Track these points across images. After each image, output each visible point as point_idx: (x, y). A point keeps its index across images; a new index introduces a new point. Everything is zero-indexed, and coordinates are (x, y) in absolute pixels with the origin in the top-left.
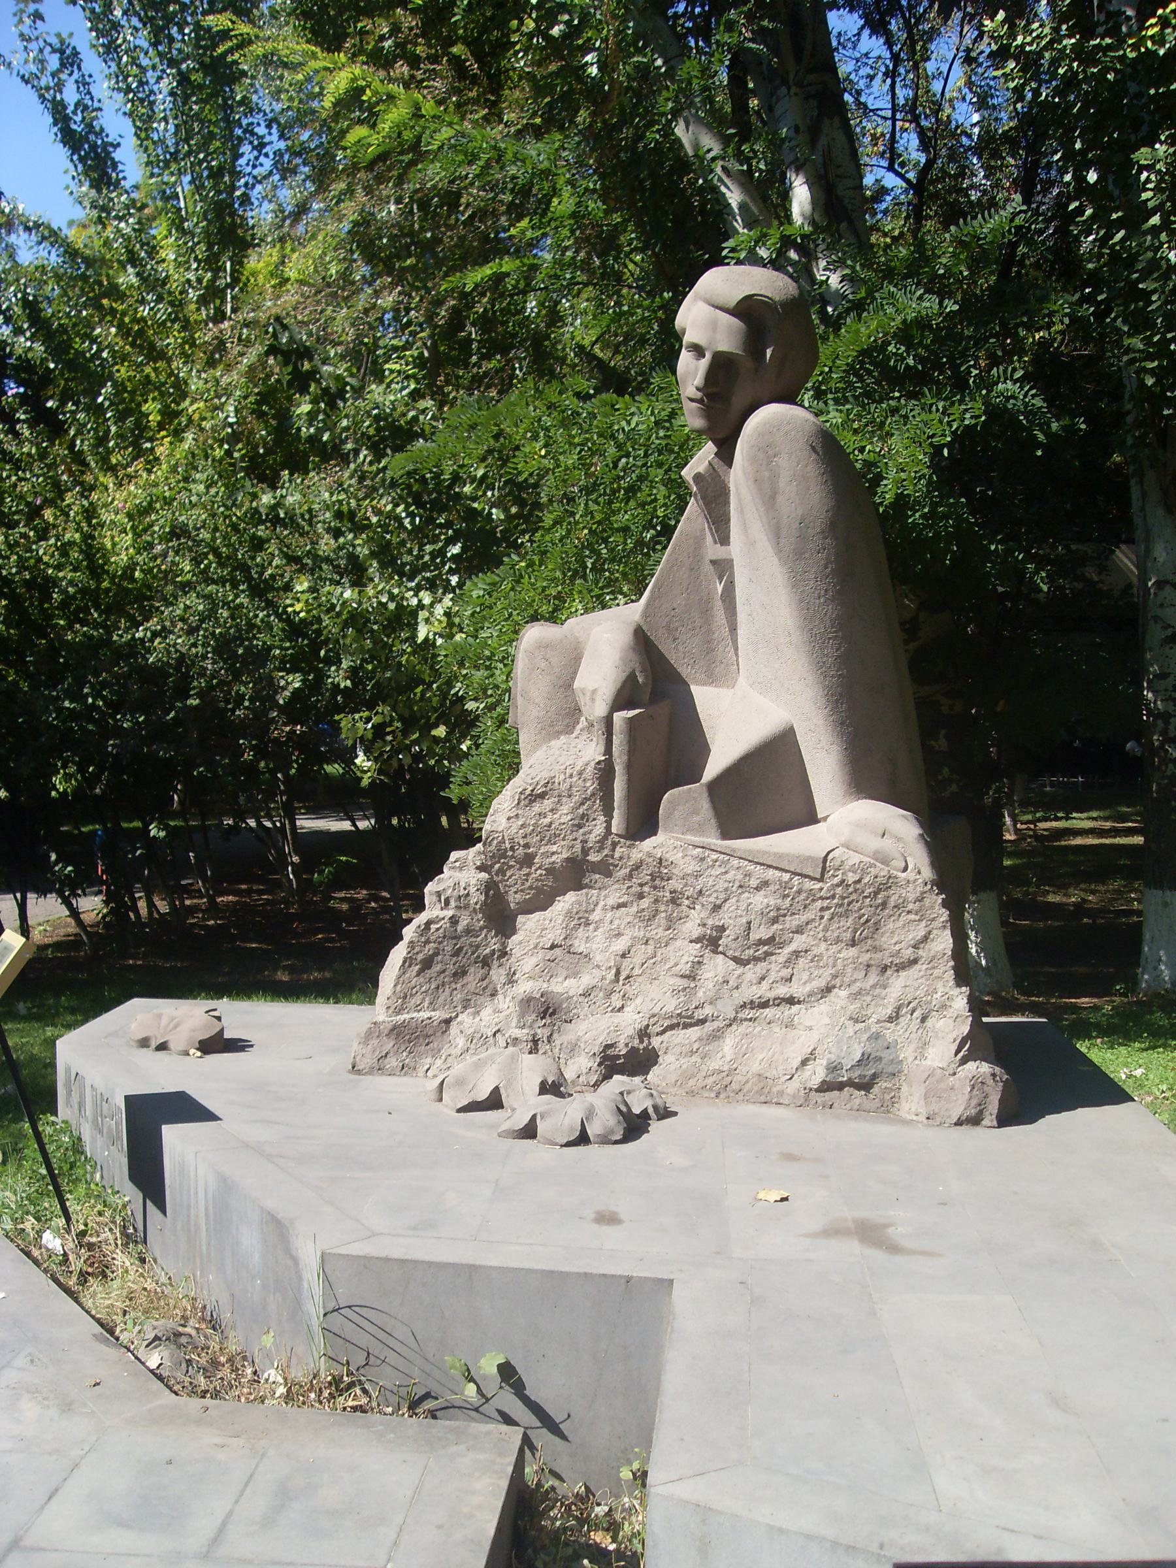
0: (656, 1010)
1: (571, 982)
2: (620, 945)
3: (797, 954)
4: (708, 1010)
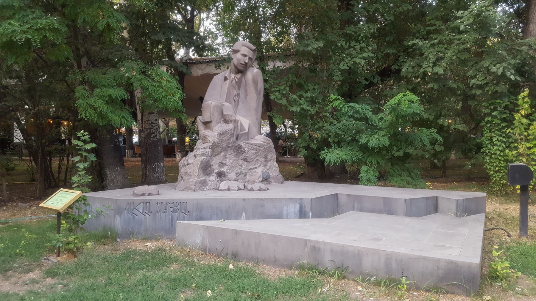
2: (231, 161)
3: (257, 160)
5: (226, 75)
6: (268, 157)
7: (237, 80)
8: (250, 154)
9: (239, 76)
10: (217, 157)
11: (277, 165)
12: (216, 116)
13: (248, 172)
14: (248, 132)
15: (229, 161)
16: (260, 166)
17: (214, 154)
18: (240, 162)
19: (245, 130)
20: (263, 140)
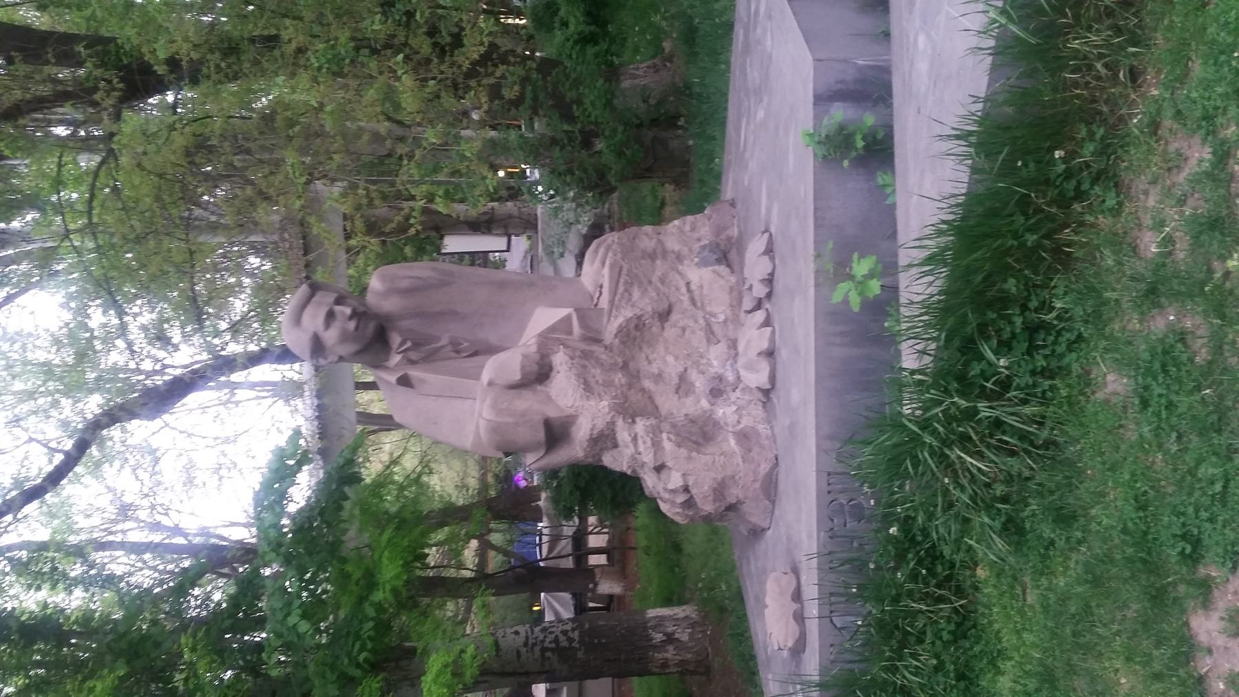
0: (705, 341)
1: (697, 384)
2: (670, 359)
4: (701, 321)
5: (393, 378)
6: (650, 250)
7: (409, 344)
8: (643, 303)
9: (395, 339)
10: (659, 401)
11: (676, 222)
12: (527, 402)
13: (703, 308)
14: (576, 310)
15: (672, 367)
16: (680, 274)
17: (651, 410)
18: (670, 332)
19: (568, 319)
20: (597, 263)
